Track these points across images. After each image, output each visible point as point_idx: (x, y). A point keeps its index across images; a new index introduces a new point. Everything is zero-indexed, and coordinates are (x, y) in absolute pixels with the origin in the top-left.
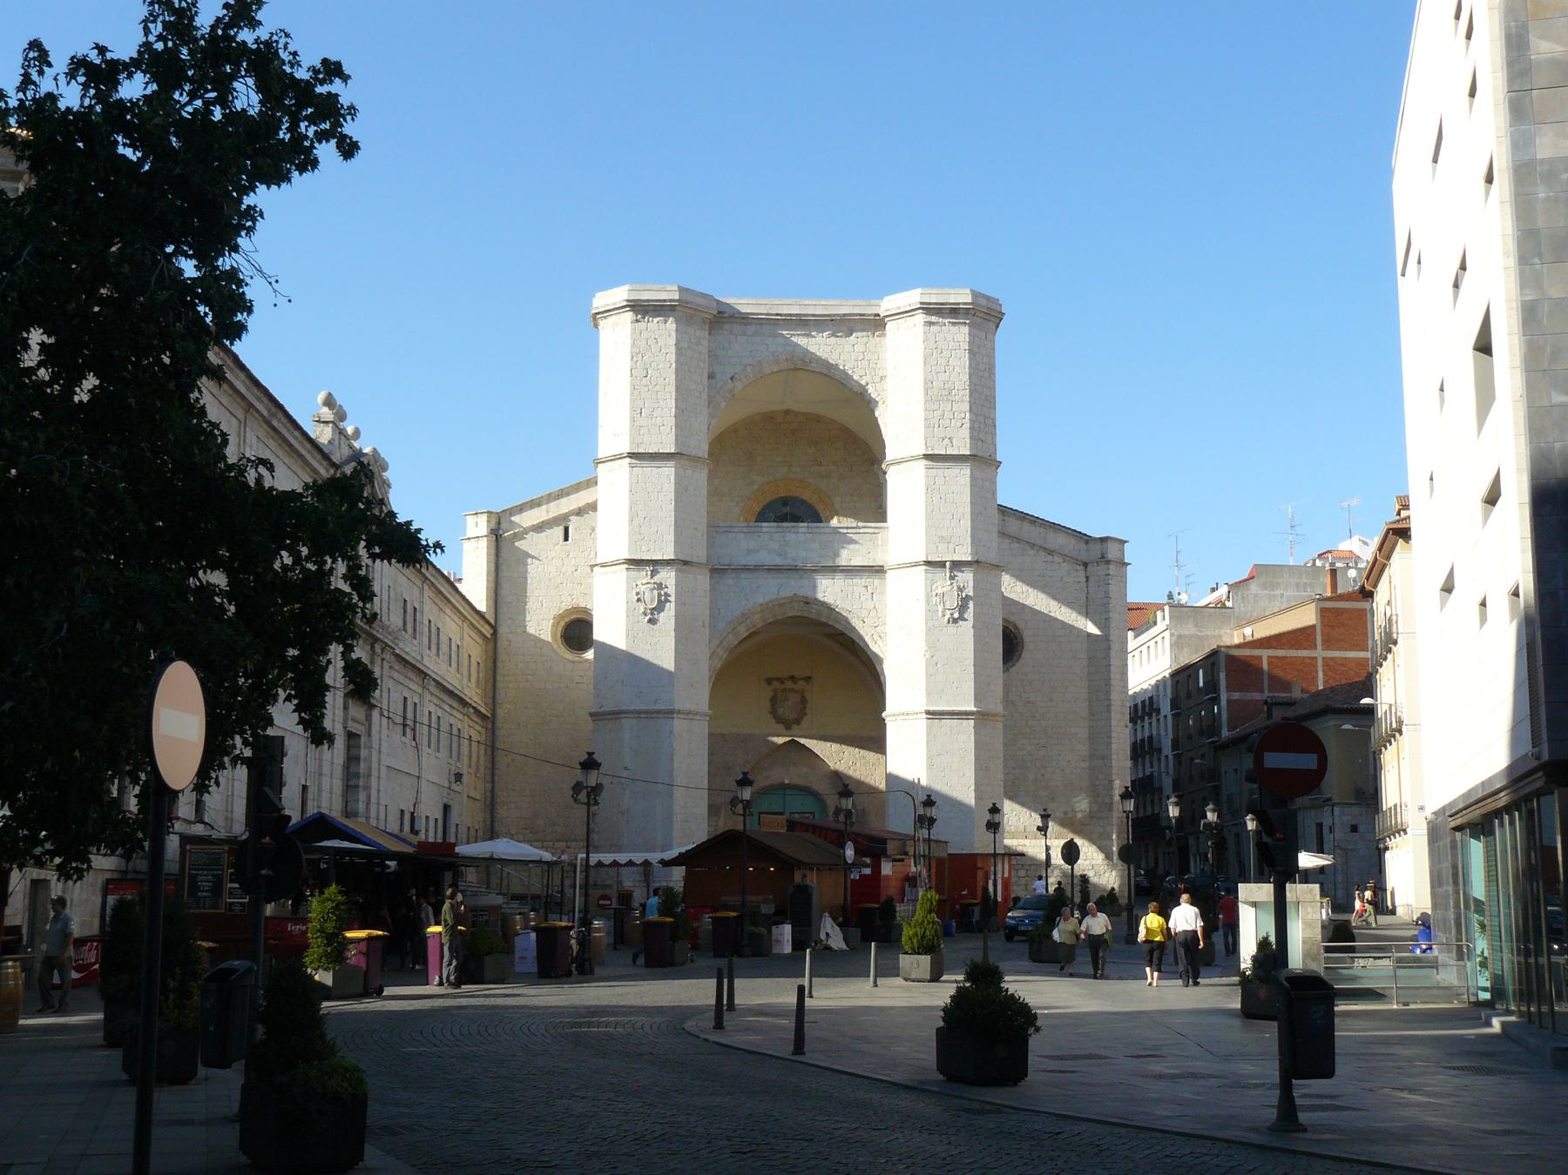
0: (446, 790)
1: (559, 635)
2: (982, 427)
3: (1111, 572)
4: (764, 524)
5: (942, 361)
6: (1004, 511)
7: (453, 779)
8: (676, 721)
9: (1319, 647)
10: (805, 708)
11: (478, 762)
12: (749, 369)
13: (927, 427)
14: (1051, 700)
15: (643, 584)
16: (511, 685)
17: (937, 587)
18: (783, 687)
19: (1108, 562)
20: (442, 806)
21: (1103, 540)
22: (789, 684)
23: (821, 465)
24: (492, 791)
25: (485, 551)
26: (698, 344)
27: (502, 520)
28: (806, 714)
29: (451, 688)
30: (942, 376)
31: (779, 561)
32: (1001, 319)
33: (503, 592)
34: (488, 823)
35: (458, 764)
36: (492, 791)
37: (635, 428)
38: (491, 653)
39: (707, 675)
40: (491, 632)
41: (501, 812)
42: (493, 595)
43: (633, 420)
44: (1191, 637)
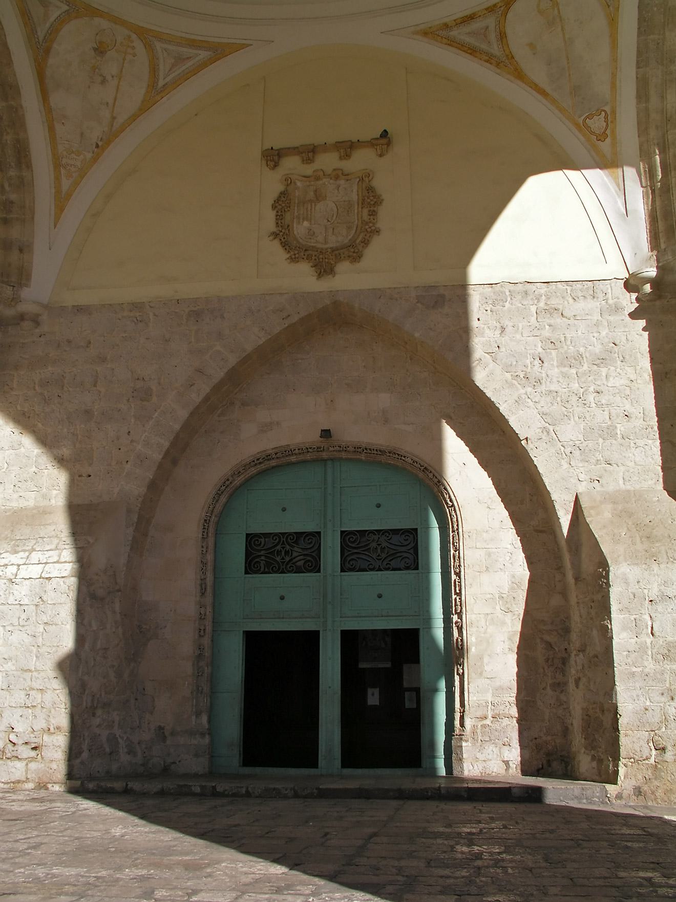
10: (373, 213)
18: (309, 170)
22: (328, 161)
28: (378, 232)
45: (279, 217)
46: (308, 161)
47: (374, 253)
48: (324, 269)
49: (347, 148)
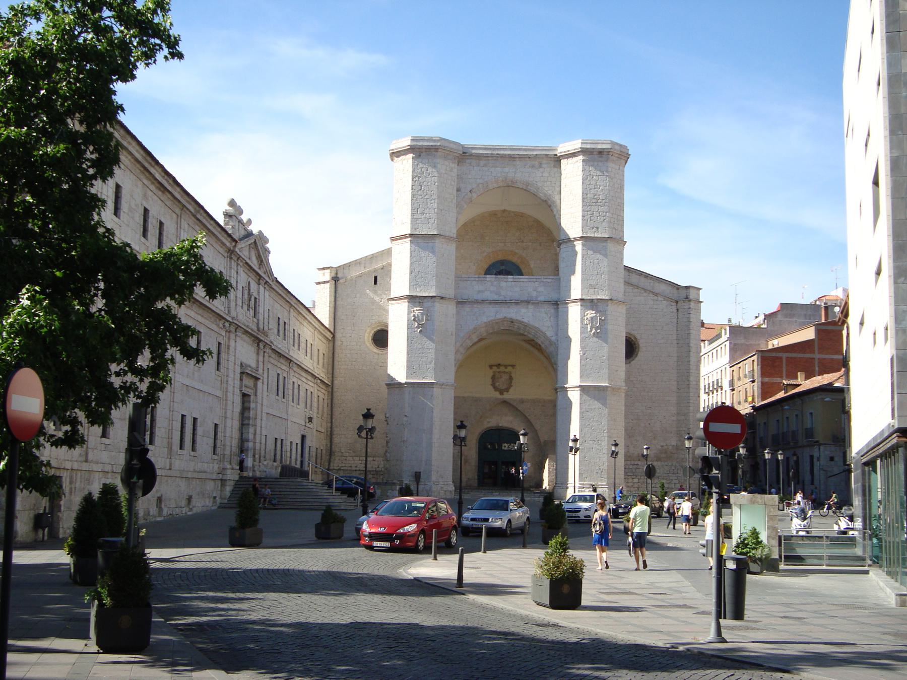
0: (303, 427)
1: (371, 338)
2: (616, 222)
3: (691, 306)
4: (488, 276)
5: (593, 183)
6: (628, 269)
7: (307, 421)
8: (435, 389)
9: (816, 351)
10: (511, 382)
11: (323, 411)
12: (480, 186)
13: (583, 220)
14: (655, 380)
15: (417, 310)
16: (342, 367)
17: (587, 314)
18: (498, 370)
19: (690, 301)
20: (300, 436)
21: (687, 288)
23: (523, 242)
24: (331, 428)
25: (328, 290)
26: (451, 171)
27: (339, 272)
29: (307, 369)
30: (593, 191)
31: (496, 297)
32: (628, 158)
33: (339, 313)
34: (329, 446)
35: (311, 412)
36: (331, 428)
37: (414, 220)
38: (331, 348)
39: (453, 363)
40: (332, 336)
41: (336, 440)
42: (333, 315)
43: (413, 215)
44: (742, 344)
45: (493, 381)
46: (498, 368)
47: (511, 390)
48: (501, 393)
49: (506, 366)
